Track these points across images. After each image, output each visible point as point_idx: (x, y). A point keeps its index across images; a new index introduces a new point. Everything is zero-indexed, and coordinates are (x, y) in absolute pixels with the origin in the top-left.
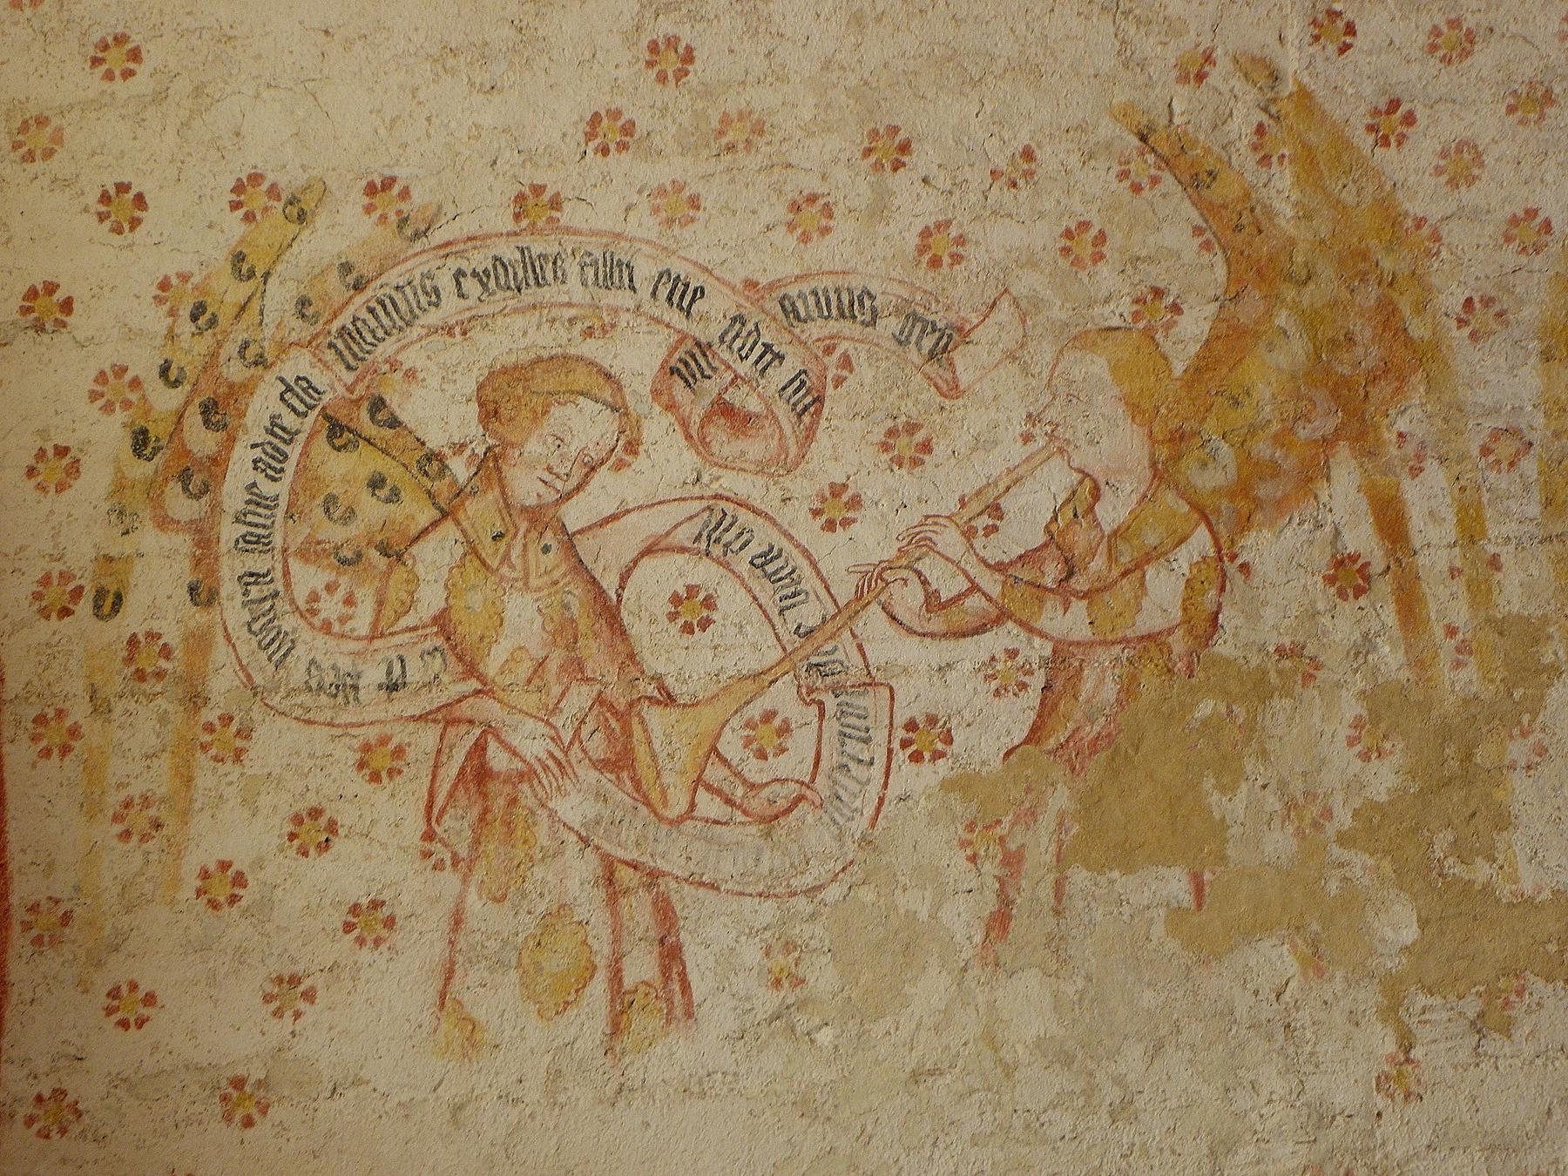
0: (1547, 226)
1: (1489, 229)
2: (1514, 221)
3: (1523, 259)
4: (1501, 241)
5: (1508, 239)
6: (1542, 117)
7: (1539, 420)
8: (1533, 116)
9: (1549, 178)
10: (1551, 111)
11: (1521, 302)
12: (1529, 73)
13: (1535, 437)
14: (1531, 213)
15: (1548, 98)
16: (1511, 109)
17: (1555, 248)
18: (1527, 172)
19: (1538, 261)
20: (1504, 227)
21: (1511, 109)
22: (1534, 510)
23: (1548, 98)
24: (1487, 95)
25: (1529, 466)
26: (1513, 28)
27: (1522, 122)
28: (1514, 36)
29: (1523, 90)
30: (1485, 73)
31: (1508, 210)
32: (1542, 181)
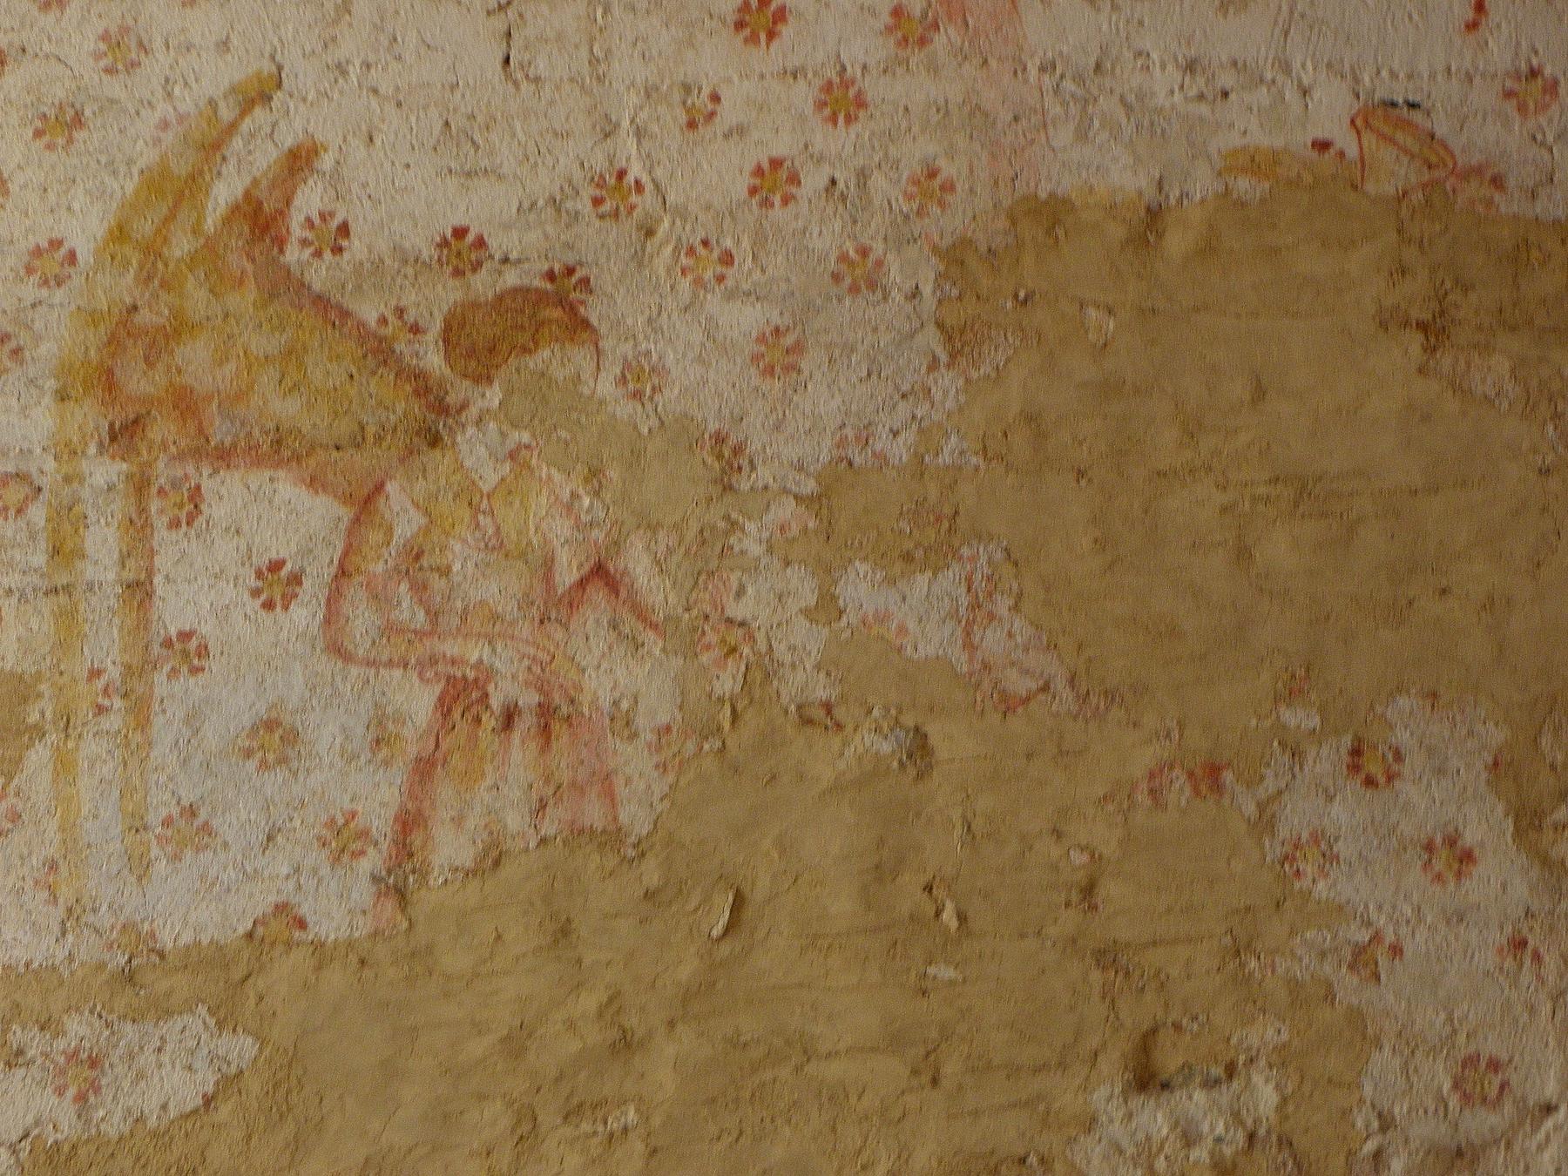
0: (72, 257)
1: (11, 261)
2: (38, 252)
3: (45, 292)
4: (22, 272)
5: (30, 270)
6: (70, 141)
7: (50, 465)
8: (61, 141)
9: (76, 206)
10: (80, 135)
11: (38, 339)
12: (61, 94)
13: (44, 482)
14: (56, 244)
15: (78, 121)
16: (38, 134)
17: (77, 281)
18: (52, 196)
19: (59, 295)
20: (26, 258)
21: (38, 134)
22: (39, 559)
23: (78, 121)
24: (14, 119)
25: (38, 514)
26: (46, 47)
27: (50, 147)
28: (47, 56)
29: (51, 113)
30: (13, 95)
31: (32, 241)
32: (69, 209)
